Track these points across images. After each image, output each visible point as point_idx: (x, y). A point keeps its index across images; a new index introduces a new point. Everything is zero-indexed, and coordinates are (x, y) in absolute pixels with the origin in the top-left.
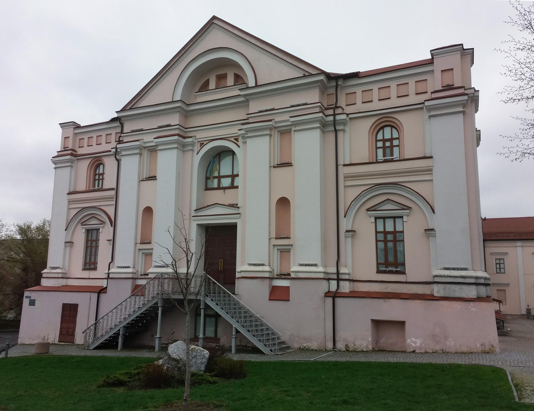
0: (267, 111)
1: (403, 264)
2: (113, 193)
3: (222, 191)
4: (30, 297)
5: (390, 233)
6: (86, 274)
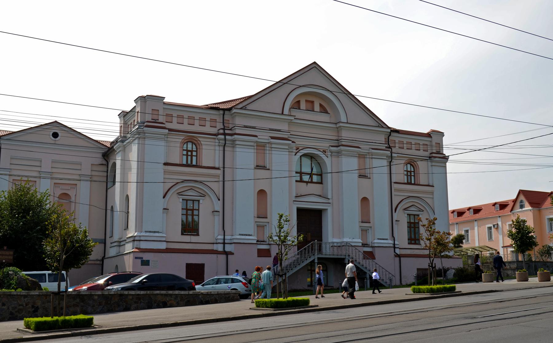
2: (219, 172)
3: (305, 184)
4: (142, 258)
6: (187, 238)
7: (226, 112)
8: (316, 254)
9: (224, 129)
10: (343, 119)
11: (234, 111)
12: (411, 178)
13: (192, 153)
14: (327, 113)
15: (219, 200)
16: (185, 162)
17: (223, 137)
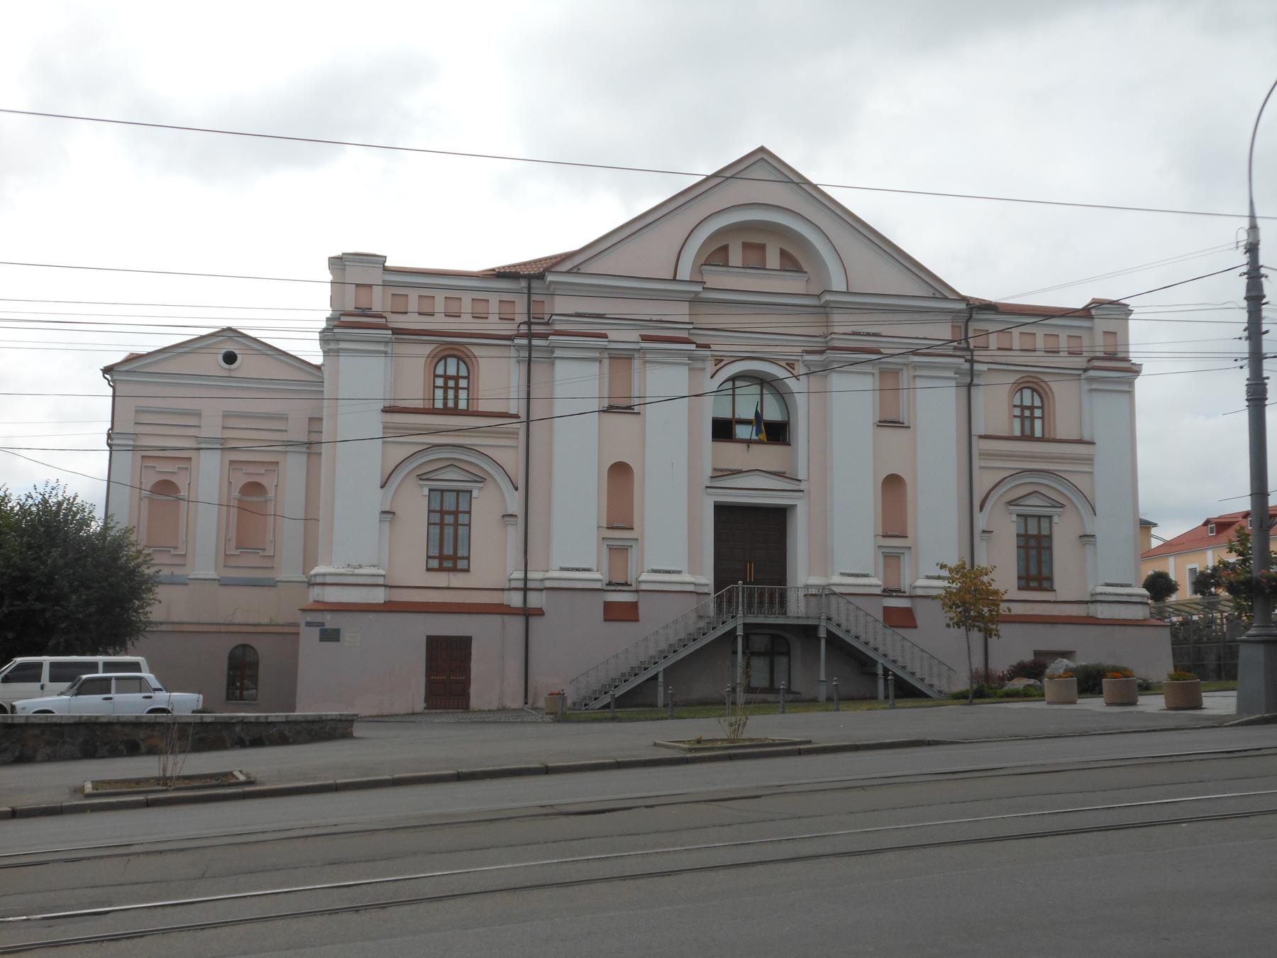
0: (868, 334)
1: (1050, 579)
3: (744, 446)
4: (322, 624)
5: (1033, 536)
6: (441, 579)
7: (535, 284)
8: (740, 614)
9: (529, 323)
10: (838, 284)
11: (550, 278)
12: (1032, 421)
13: (457, 384)
14: (800, 270)
15: (516, 489)
16: (439, 404)
17: (525, 342)
